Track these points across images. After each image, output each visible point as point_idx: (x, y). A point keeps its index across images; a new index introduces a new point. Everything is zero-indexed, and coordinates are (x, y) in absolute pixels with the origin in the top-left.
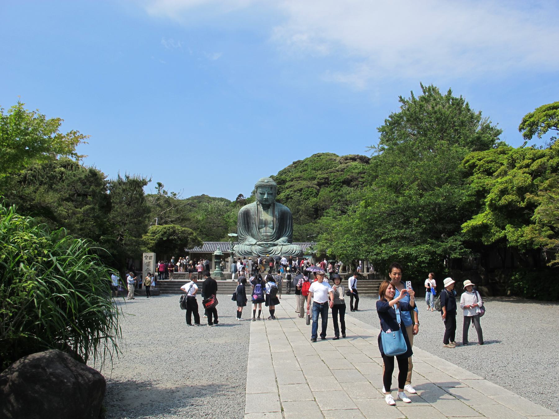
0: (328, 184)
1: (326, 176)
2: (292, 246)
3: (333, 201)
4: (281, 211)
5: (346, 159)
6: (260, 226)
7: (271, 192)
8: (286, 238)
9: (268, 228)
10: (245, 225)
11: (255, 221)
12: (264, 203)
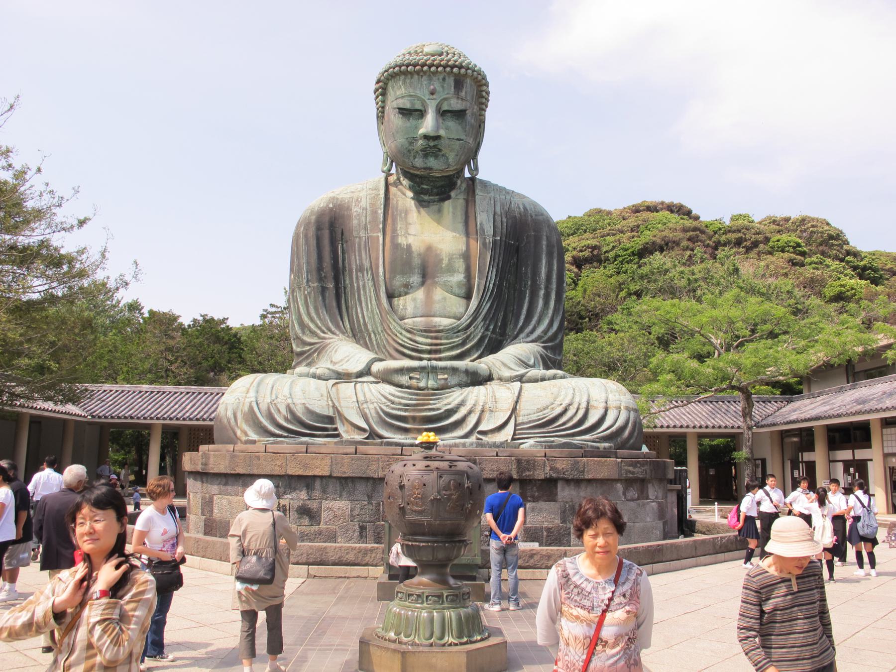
0: (600, 261)
1: (593, 242)
3: (622, 294)
4: (508, 213)
5: (636, 210)
6: (399, 280)
7: (455, 104)
8: (536, 347)
9: (439, 294)
10: (321, 279)
12: (419, 162)
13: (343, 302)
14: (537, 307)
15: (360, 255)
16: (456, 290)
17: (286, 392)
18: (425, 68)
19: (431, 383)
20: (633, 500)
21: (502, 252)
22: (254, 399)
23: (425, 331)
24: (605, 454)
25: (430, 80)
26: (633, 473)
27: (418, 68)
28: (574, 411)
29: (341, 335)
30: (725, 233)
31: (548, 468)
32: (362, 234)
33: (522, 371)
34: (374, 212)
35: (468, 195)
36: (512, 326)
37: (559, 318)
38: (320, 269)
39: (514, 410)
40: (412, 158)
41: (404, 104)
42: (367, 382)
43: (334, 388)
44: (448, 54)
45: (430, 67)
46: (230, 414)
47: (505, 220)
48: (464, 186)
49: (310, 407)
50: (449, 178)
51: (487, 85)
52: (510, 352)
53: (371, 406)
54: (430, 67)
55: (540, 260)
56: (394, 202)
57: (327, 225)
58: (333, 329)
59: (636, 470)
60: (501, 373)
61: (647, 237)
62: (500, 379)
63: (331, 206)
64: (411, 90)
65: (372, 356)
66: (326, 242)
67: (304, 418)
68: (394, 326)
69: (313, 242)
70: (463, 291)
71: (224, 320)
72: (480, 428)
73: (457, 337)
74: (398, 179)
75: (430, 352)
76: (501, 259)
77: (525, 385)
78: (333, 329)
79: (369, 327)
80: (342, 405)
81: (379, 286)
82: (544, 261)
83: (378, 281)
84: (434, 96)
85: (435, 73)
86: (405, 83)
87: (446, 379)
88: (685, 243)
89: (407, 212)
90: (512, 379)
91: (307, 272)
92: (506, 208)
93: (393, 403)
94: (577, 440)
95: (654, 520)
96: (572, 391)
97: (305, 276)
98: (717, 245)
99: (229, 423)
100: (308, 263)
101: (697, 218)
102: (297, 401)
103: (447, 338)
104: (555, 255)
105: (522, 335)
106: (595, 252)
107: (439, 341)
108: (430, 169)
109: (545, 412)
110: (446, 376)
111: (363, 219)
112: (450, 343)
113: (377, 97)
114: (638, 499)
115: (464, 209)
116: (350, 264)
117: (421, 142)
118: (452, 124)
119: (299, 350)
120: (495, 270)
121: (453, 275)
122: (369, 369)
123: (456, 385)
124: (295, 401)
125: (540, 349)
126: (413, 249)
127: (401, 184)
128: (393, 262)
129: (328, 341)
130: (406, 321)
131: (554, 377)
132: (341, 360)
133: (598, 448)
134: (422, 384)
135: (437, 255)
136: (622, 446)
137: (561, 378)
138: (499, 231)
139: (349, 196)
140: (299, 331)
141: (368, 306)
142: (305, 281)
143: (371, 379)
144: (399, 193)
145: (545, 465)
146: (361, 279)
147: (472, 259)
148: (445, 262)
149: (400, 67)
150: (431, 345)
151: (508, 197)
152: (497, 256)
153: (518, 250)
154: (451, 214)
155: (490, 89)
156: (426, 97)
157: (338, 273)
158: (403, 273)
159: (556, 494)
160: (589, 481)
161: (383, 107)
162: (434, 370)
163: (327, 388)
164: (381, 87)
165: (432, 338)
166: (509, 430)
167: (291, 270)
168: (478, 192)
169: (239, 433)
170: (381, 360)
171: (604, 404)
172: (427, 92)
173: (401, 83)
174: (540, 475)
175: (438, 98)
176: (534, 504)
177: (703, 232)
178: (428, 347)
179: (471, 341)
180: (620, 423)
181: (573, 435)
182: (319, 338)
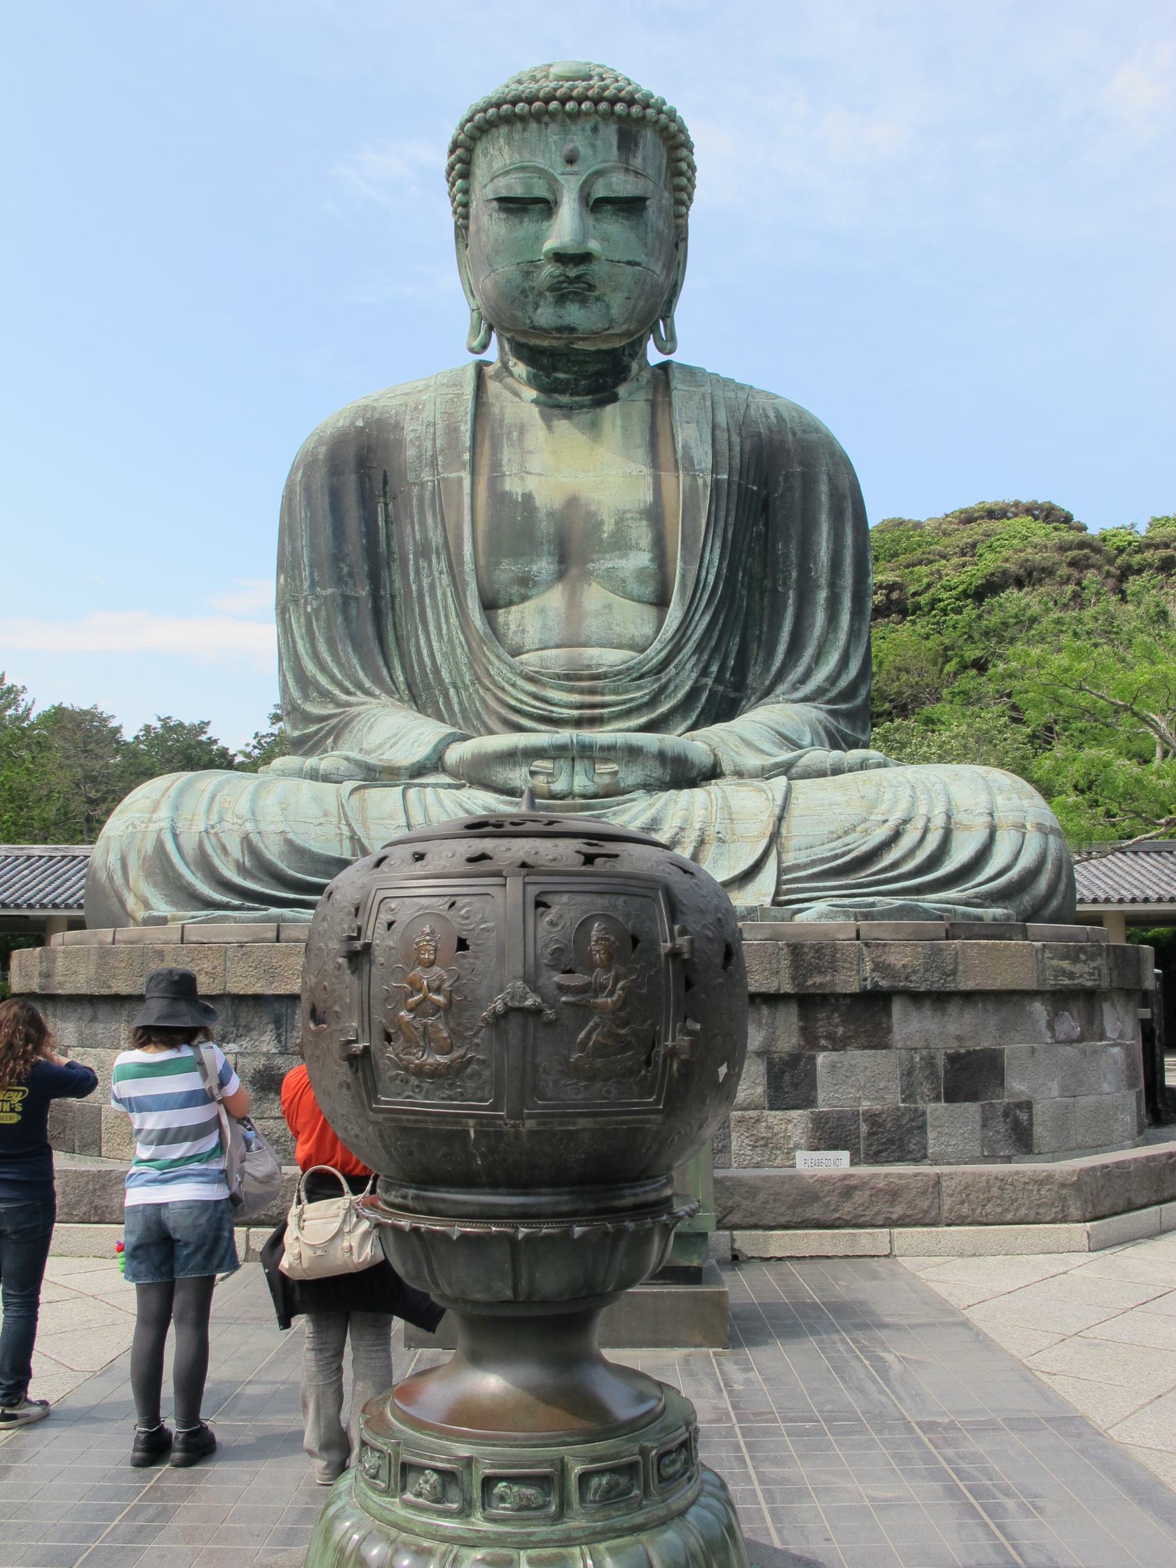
0: (904, 613)
2: (910, 772)
3: (950, 667)
4: (743, 425)
5: (968, 518)
6: (507, 570)
7: (622, 185)
8: (814, 713)
9: (595, 596)
10: (340, 580)
11: (446, 523)
12: (545, 315)
13: (390, 627)
14: (812, 625)
15: (423, 523)
16: (634, 587)
17: (243, 806)
18: (554, 105)
19: (581, 782)
20: (1070, 1041)
21: (733, 507)
22: (166, 824)
23: (568, 677)
24: (998, 931)
25: (565, 131)
26: (1071, 976)
27: (537, 104)
28: (917, 835)
29: (384, 697)
30: (1139, 550)
31: (869, 966)
32: (426, 476)
33: (785, 756)
34: (452, 430)
35: (655, 392)
36: (758, 669)
37: (862, 650)
38: (338, 558)
40: (530, 308)
41: (509, 187)
42: (436, 786)
43: (356, 797)
45: (563, 101)
46: (113, 860)
47: (736, 439)
48: (646, 376)
49: (298, 841)
50: (613, 354)
51: (688, 146)
52: (757, 718)
54: (563, 101)
56: (496, 410)
57: (352, 465)
58: (368, 684)
59: (1078, 968)
60: (738, 760)
61: (989, 563)
62: (739, 774)
63: (360, 423)
64: (527, 156)
65: (447, 729)
66: (351, 500)
67: (282, 865)
68: (497, 668)
70: (648, 591)
71: (202, 727)
73: (639, 688)
74: (505, 365)
75: (578, 723)
76: (731, 520)
77: (799, 784)
78: (368, 684)
79: (445, 674)
80: (372, 834)
81: (465, 583)
82: (825, 528)
83: (462, 572)
84: (575, 168)
85: (575, 116)
86: (509, 141)
87: (616, 773)
88: (1064, 571)
90: (766, 773)
91: (311, 566)
92: (739, 417)
94: (930, 901)
95: (1118, 1090)
96: (909, 792)
97: (306, 573)
98: (1127, 572)
99: (111, 879)
100: (313, 546)
101: (1083, 528)
102: (266, 827)
103: (615, 692)
104: (849, 514)
105: (781, 688)
106: (895, 595)
107: (597, 699)
108: (571, 329)
109: (847, 839)
111: (428, 444)
112: (624, 702)
113: (453, 185)
114: (1081, 1039)
115: (648, 419)
116: (402, 546)
117: (549, 270)
118: (614, 226)
119: (296, 733)
120: (718, 544)
121: (624, 556)
122: (441, 758)
123: (637, 787)
124: (262, 827)
125: (822, 715)
126: (539, 502)
127: (511, 374)
128: (494, 531)
129: (354, 710)
130: (524, 657)
131: (863, 766)
132: (381, 745)
133: (980, 918)
134: (559, 786)
135: (590, 515)
136: (1034, 914)
137: (879, 765)
138: (724, 462)
139: (397, 402)
140: (295, 693)
141: (441, 632)
142: (306, 585)
143: (446, 779)
144: (507, 394)
145: (861, 959)
146: (425, 572)
148: (608, 527)
149: (498, 105)
150: (581, 706)
151: (742, 396)
152: (722, 514)
153: (766, 506)
154: (618, 431)
155: (697, 159)
156: (558, 169)
157: (377, 562)
159: (889, 1030)
160: (968, 996)
161: (466, 205)
162: (587, 753)
163: (338, 796)
164: (460, 160)
165: (582, 691)
166: (766, 881)
167: (281, 567)
168: (675, 383)
169: (131, 902)
170: (465, 738)
171: (986, 819)
172: (558, 159)
173: (501, 140)
174: (849, 982)
175: (584, 170)
176: (834, 1056)
177: (1097, 550)
178: (576, 713)
179: (669, 696)
180: (1026, 860)
181: (919, 890)
182: (339, 704)
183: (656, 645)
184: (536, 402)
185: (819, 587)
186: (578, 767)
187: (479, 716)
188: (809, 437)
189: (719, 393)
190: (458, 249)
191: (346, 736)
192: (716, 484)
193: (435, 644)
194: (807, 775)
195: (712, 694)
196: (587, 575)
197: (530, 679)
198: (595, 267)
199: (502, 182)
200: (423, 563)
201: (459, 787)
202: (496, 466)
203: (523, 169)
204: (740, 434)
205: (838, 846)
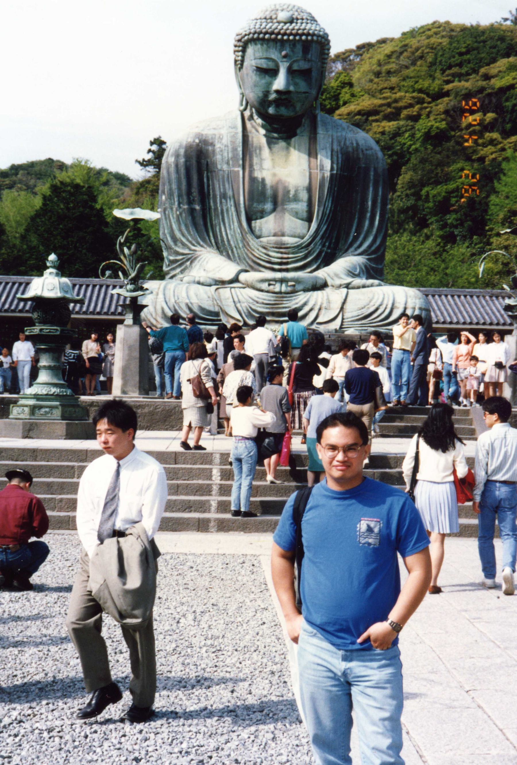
7: (303, 65)
10: (190, 202)
12: (271, 110)
15: (224, 185)
17: (184, 294)
18: (279, 37)
27: (273, 36)
29: (208, 249)
33: (349, 280)
37: (382, 235)
38: (189, 193)
39: (342, 309)
44: (297, 19)
47: (340, 156)
49: (203, 306)
53: (243, 305)
55: (368, 188)
62: (333, 286)
69: (183, 171)
72: (319, 320)
75: (280, 264)
77: (350, 291)
78: (202, 243)
79: (232, 243)
81: (241, 211)
82: (371, 189)
87: (294, 286)
89: (260, 149)
90: (340, 286)
93: (257, 302)
100: (179, 188)
102: (193, 301)
103: (293, 253)
104: (381, 183)
110: (293, 283)
111: (225, 154)
116: (214, 191)
119: (171, 258)
130: (262, 239)
131: (372, 285)
132: (214, 270)
134: (277, 289)
144: (254, 131)
146: (224, 204)
147: (313, 188)
148: (292, 193)
150: (282, 258)
151: (344, 134)
157: (204, 196)
158: (259, 202)
161: (243, 61)
165: (282, 253)
178: (279, 260)
179: (311, 255)
182: (190, 249)
183: (307, 237)
184: (265, 135)
185: (367, 211)
186: (284, 285)
187: (245, 259)
188: (368, 152)
189: (335, 134)
190: (236, 69)
191: (196, 262)
192: (332, 175)
193: (228, 231)
194: (353, 288)
195: (326, 253)
196: (284, 210)
197: (264, 248)
198: (292, 95)
199: (259, 61)
200: (223, 201)
201: (244, 288)
202: (251, 166)
203: (267, 58)
204: (342, 153)
205: (360, 312)
